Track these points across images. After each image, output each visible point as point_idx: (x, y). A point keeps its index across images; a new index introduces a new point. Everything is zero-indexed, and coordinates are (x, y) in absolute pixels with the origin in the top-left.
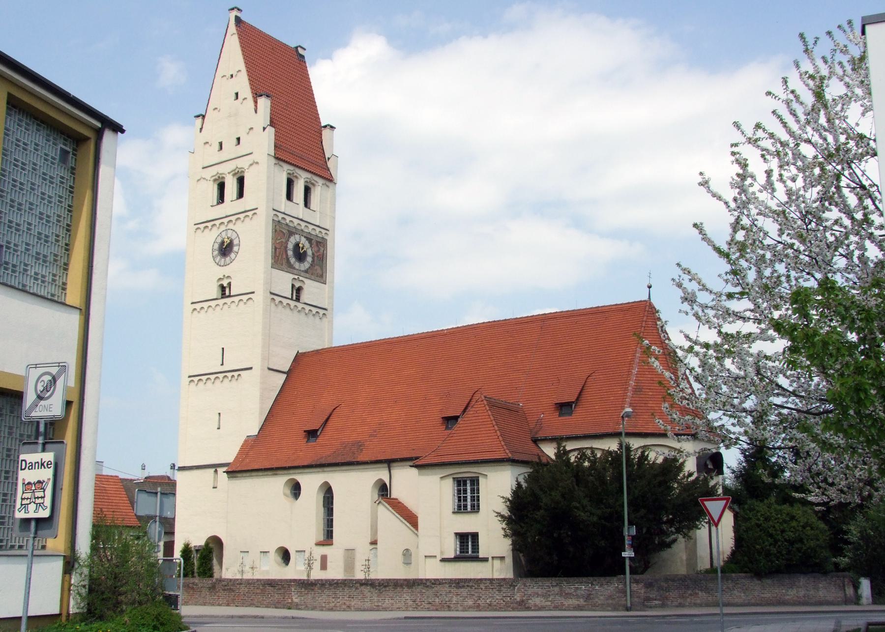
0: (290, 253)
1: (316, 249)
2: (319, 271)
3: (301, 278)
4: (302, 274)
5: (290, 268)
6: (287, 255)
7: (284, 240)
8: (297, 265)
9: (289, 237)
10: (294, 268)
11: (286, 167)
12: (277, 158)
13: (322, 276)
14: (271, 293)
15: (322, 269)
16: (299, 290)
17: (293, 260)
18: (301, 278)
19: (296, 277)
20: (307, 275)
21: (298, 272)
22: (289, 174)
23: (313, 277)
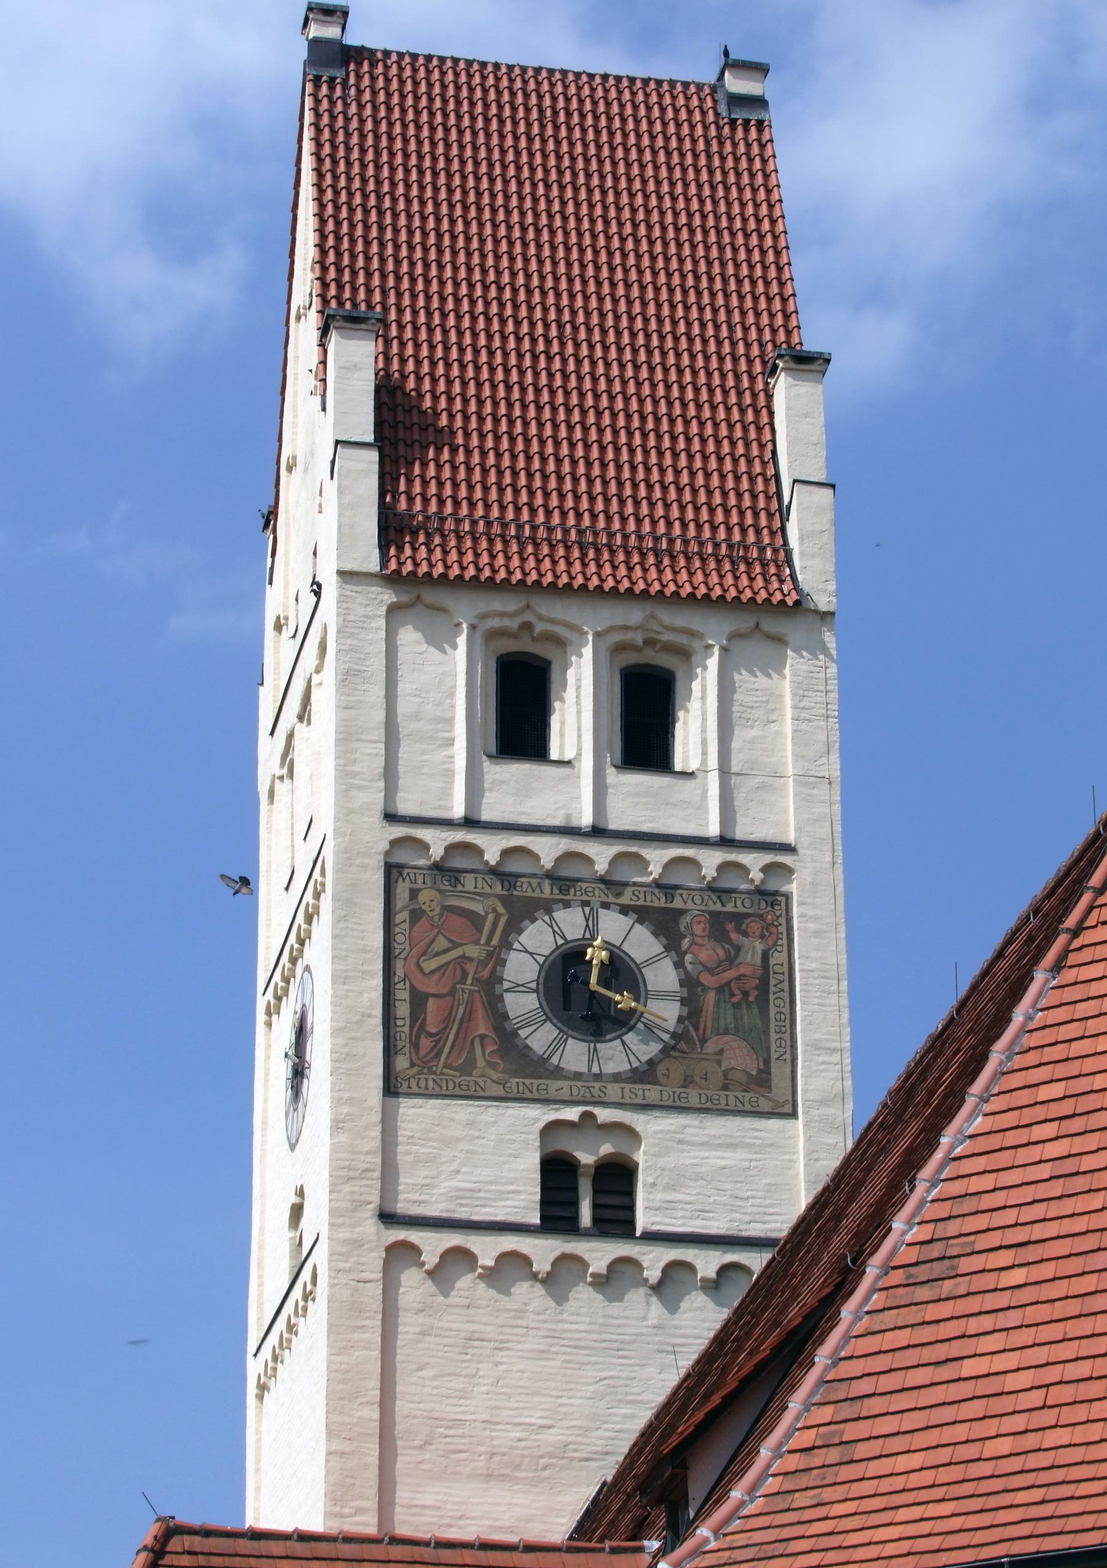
0: (521, 1004)
1: (711, 952)
2: (740, 1057)
3: (604, 1115)
4: (613, 1091)
5: (521, 1072)
6: (499, 1017)
7: (472, 951)
8: (575, 1055)
9: (514, 927)
10: (558, 1073)
11: (465, 608)
12: (393, 579)
13: (762, 1080)
14: (387, 1218)
15: (759, 1043)
16: (617, 1178)
17: (540, 1038)
18: (604, 1115)
19: (572, 1114)
20: (653, 1093)
21: (590, 1087)
22: (493, 635)
23: (731, 1098)
